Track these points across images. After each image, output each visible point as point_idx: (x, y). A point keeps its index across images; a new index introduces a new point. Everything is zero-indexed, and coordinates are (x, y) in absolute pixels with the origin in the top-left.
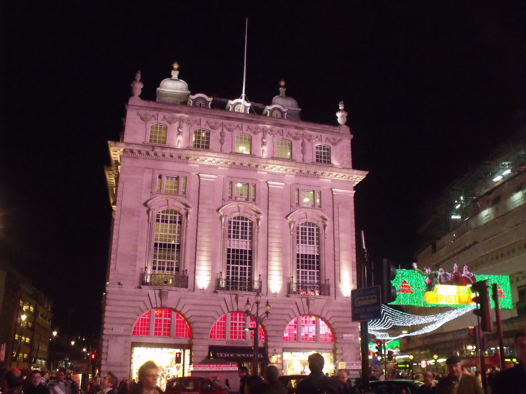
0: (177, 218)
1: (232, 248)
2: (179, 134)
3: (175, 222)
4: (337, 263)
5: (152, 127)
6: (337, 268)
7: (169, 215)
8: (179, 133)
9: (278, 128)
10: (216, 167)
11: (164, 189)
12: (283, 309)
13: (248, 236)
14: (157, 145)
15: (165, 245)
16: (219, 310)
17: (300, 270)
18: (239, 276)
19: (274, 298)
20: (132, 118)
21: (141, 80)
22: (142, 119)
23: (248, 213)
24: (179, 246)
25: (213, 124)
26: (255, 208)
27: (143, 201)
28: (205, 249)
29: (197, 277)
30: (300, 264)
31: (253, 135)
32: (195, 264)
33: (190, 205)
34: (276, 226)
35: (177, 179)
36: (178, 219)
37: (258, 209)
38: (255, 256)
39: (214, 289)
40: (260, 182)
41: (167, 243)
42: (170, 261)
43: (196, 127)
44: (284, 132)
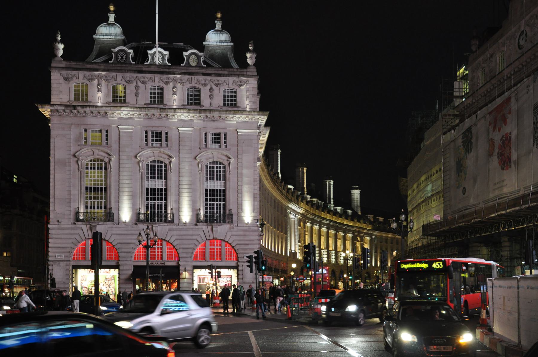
0: (103, 165)
1: (150, 187)
2: (98, 91)
3: (101, 169)
4: (240, 195)
5: (75, 86)
6: (240, 199)
7: (96, 163)
8: (99, 90)
9: (187, 77)
11: (90, 140)
12: (192, 235)
13: (163, 176)
14: (80, 102)
15: (94, 188)
17: (209, 203)
18: (156, 210)
19: (184, 227)
20: (56, 77)
23: (162, 157)
24: (105, 188)
25: (128, 79)
27: (72, 153)
30: (208, 198)
31: (164, 86)
32: (118, 202)
33: (111, 154)
34: (186, 167)
35: (100, 131)
36: (102, 165)
37: (170, 153)
38: (169, 193)
39: (134, 222)
41: (96, 186)
42: (100, 201)
43: (114, 83)
44: (193, 79)
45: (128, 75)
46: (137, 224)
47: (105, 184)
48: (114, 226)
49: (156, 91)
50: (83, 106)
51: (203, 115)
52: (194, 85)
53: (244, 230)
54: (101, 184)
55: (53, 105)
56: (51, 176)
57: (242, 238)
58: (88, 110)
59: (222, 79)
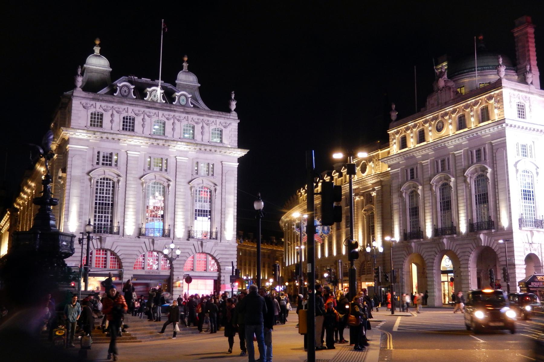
4: (223, 216)
5: (92, 114)
6: (223, 220)
10: (140, 146)
15: (102, 203)
16: (141, 250)
19: (179, 241)
22: (84, 107)
24: (112, 205)
25: (137, 112)
26: (167, 177)
28: (131, 206)
29: (125, 227)
31: (166, 121)
41: (104, 202)
46: (139, 238)
47: (112, 201)
48: (120, 238)
54: (109, 201)
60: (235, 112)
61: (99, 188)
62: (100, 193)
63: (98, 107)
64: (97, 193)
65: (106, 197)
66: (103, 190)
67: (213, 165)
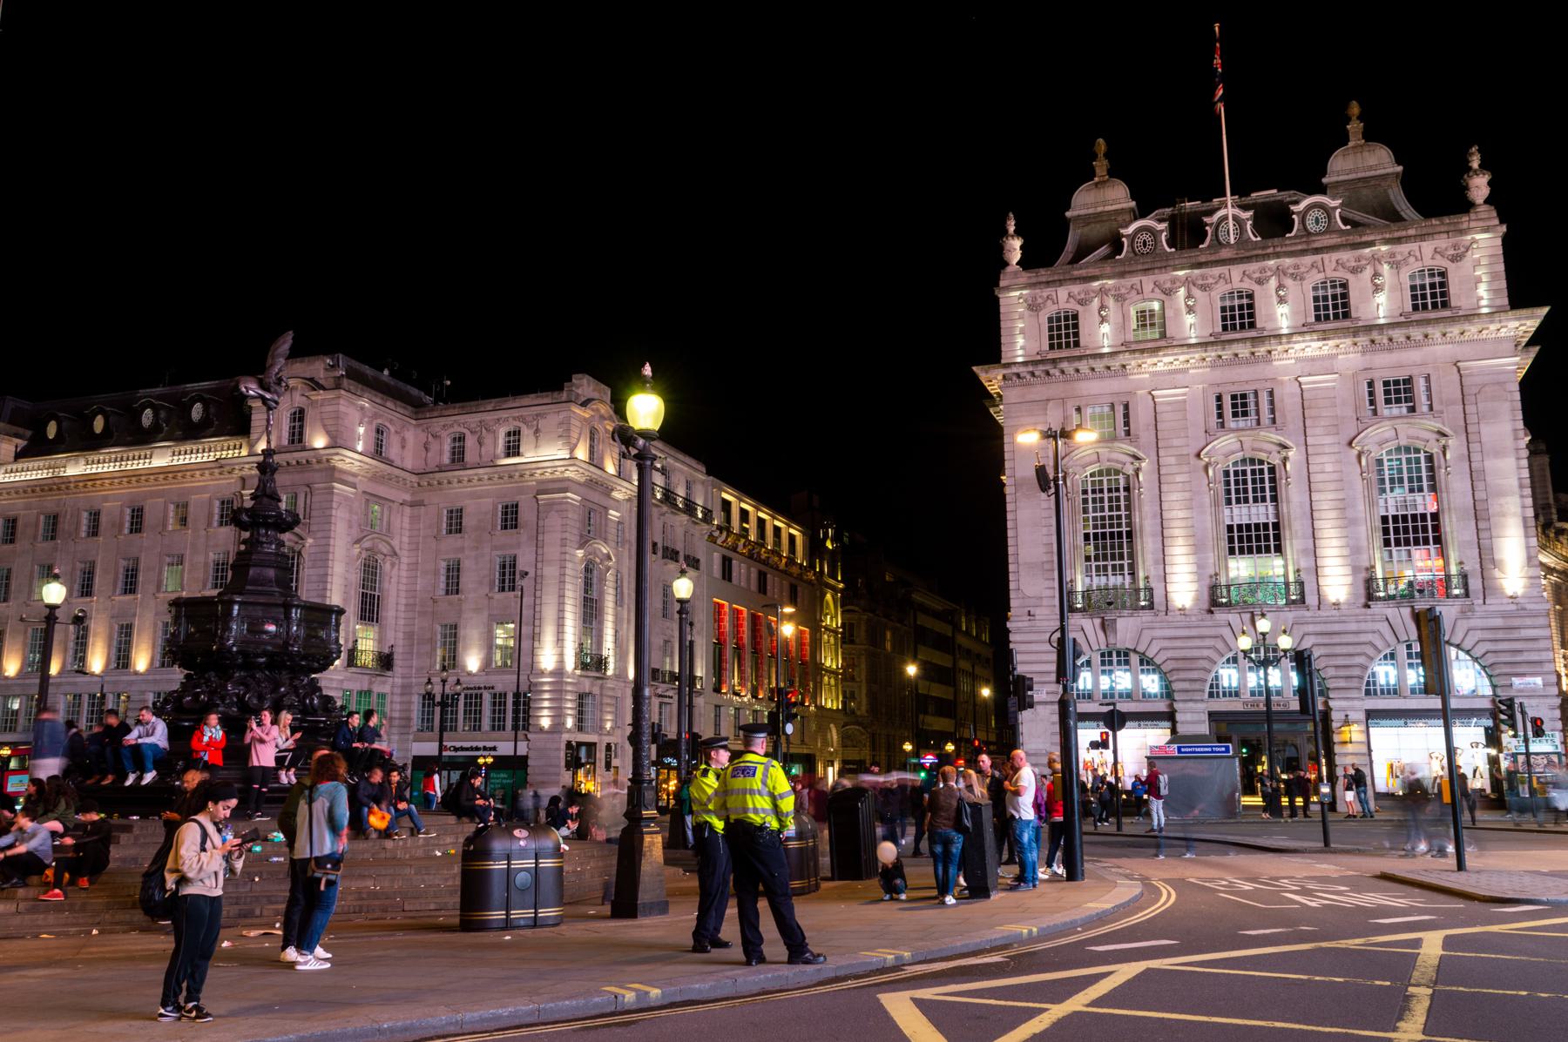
1: (1236, 522)
5: (1050, 320)
8: (1103, 320)
13: (1268, 494)
15: (1104, 534)
21: (1018, 233)
24: (1130, 534)
25: (1168, 285)
33: (1141, 454)
34: (1325, 466)
37: (1282, 439)
38: (1286, 534)
39: (1206, 606)
40: (1282, 383)
45: (1164, 278)
47: (1129, 524)
49: (1236, 302)
50: (1070, 359)
51: (1363, 340)
52: (1331, 274)
53: (1505, 615)
55: (1008, 365)
56: (1009, 516)
57: (1500, 635)
58: (1083, 366)
59: (1404, 248)
60: (1486, 207)
61: (1090, 496)
62: (1095, 510)
63: (1063, 298)
64: (1085, 511)
65: (1111, 518)
66: (1102, 500)
67: (1428, 379)
